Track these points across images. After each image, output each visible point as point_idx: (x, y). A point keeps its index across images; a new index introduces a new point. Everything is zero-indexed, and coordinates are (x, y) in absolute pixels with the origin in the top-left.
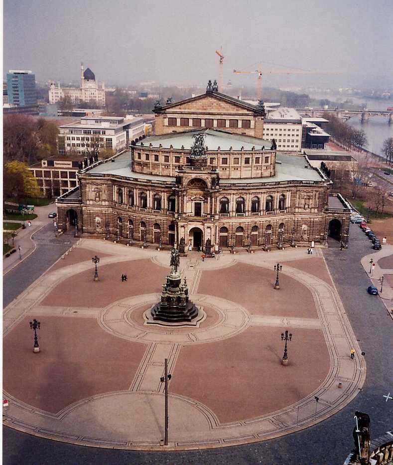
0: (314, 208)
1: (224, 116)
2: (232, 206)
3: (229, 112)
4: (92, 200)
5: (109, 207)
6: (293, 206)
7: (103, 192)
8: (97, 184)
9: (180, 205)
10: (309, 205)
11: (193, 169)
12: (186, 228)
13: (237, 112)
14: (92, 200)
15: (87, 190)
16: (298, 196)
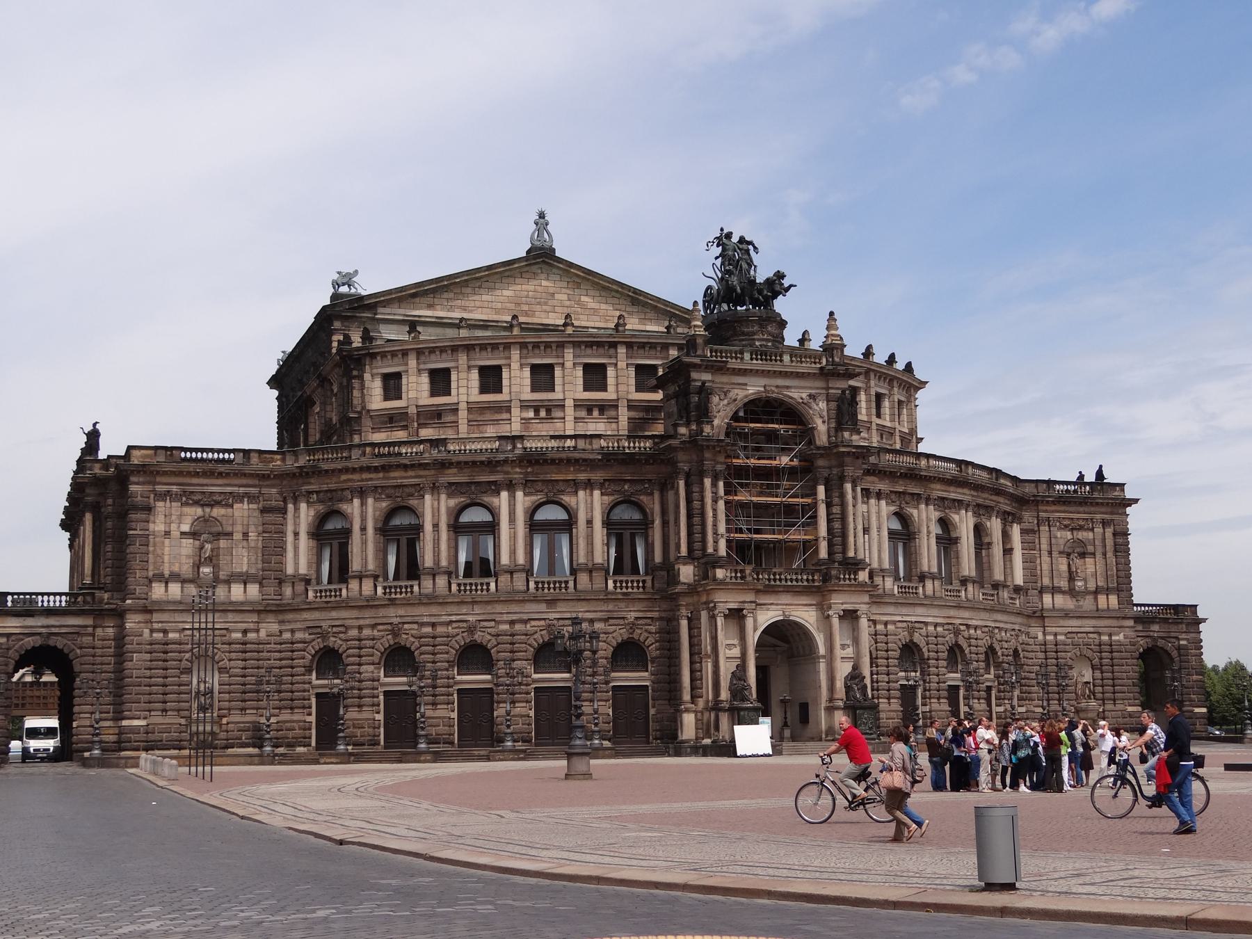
0: (1108, 591)
4: (175, 577)
7: (238, 536)
8: (210, 501)
9: (710, 514)
10: (1085, 580)
11: (747, 356)
12: (749, 622)
15: (158, 526)
16: (1045, 546)
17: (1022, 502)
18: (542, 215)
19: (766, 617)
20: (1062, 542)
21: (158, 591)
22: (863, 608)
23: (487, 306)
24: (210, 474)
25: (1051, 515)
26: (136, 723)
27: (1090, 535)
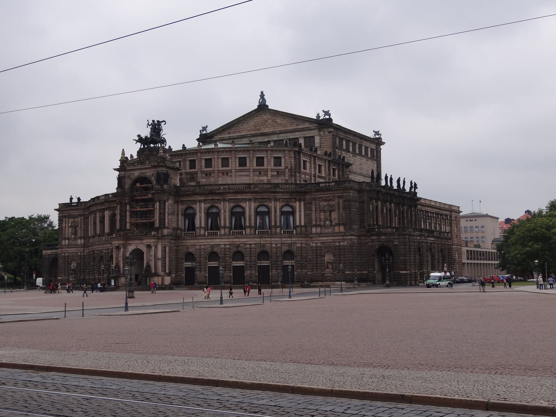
0: (338, 225)
1: (281, 135)
2: (200, 220)
3: (286, 128)
4: (68, 239)
5: (84, 246)
6: (309, 224)
7: (80, 226)
8: (74, 217)
10: (331, 221)
11: (136, 164)
12: (122, 250)
13: (297, 127)
14: (68, 239)
15: (64, 225)
16: (314, 209)
17: (305, 193)
18: (262, 93)
19: (131, 248)
20: (322, 207)
21: (63, 243)
22: (152, 244)
23: (245, 129)
24: (72, 210)
25: (317, 197)
26: (60, 278)
27: (334, 203)
